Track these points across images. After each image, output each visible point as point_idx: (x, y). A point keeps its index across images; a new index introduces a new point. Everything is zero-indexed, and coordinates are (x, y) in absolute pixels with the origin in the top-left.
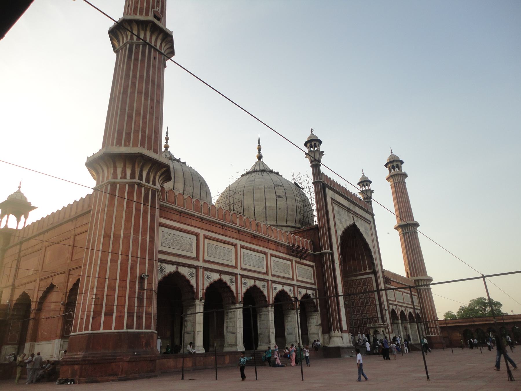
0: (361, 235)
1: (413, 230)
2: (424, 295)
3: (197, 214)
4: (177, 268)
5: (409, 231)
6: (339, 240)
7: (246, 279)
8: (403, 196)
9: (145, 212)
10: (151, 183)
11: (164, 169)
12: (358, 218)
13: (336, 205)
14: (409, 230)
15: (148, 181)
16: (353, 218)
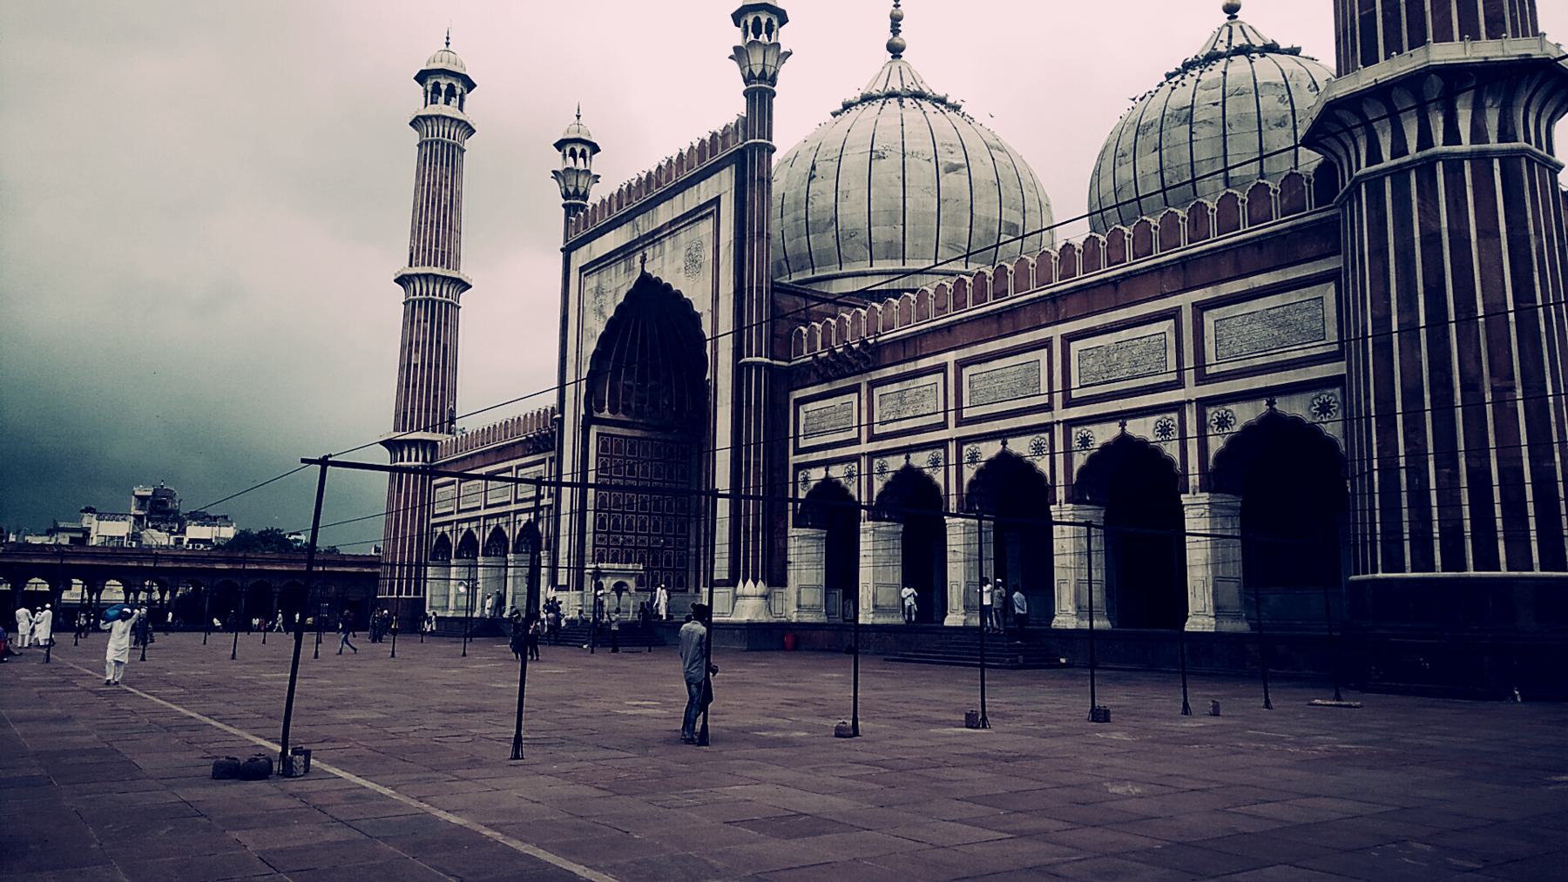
12: (662, 240)
16: (643, 260)
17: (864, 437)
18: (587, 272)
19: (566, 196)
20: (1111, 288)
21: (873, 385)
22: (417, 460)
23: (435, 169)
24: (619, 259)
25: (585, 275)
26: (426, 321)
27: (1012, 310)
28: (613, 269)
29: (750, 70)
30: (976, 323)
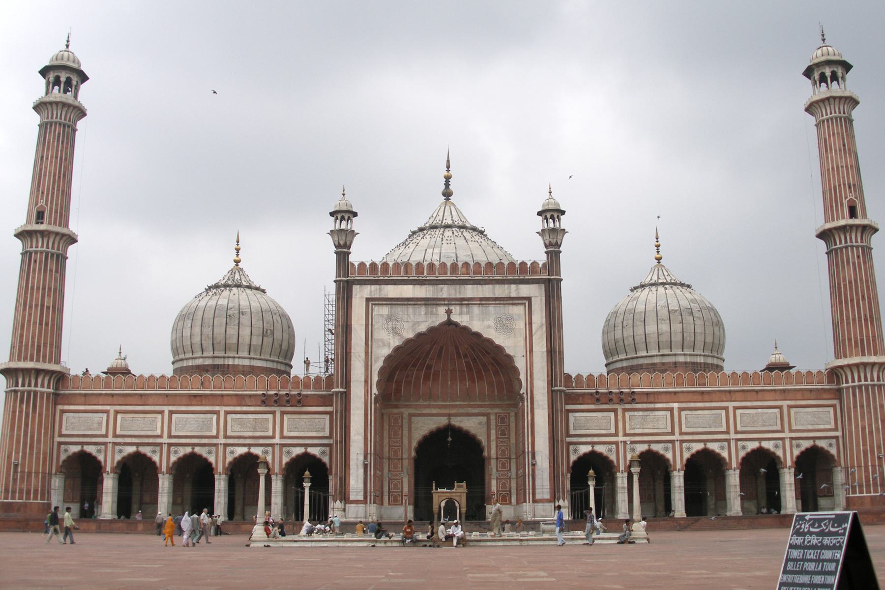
0: (478, 335)
1: (843, 242)
2: (849, 403)
3: (104, 392)
4: (82, 447)
5: (834, 247)
6: (378, 365)
7: (179, 447)
8: (827, 158)
9: (21, 412)
10: (26, 386)
11: (33, 372)
12: (470, 306)
13: (384, 306)
14: (833, 245)
15: (23, 385)
16: (449, 312)
17: (621, 433)
18: (377, 303)
19: (338, 246)
20: (755, 393)
21: (625, 410)
22: (49, 387)
23: (67, 148)
24: (421, 305)
25: (373, 304)
26: (56, 271)
27: (709, 392)
28: (411, 309)
29: (557, 241)
30: (690, 394)
